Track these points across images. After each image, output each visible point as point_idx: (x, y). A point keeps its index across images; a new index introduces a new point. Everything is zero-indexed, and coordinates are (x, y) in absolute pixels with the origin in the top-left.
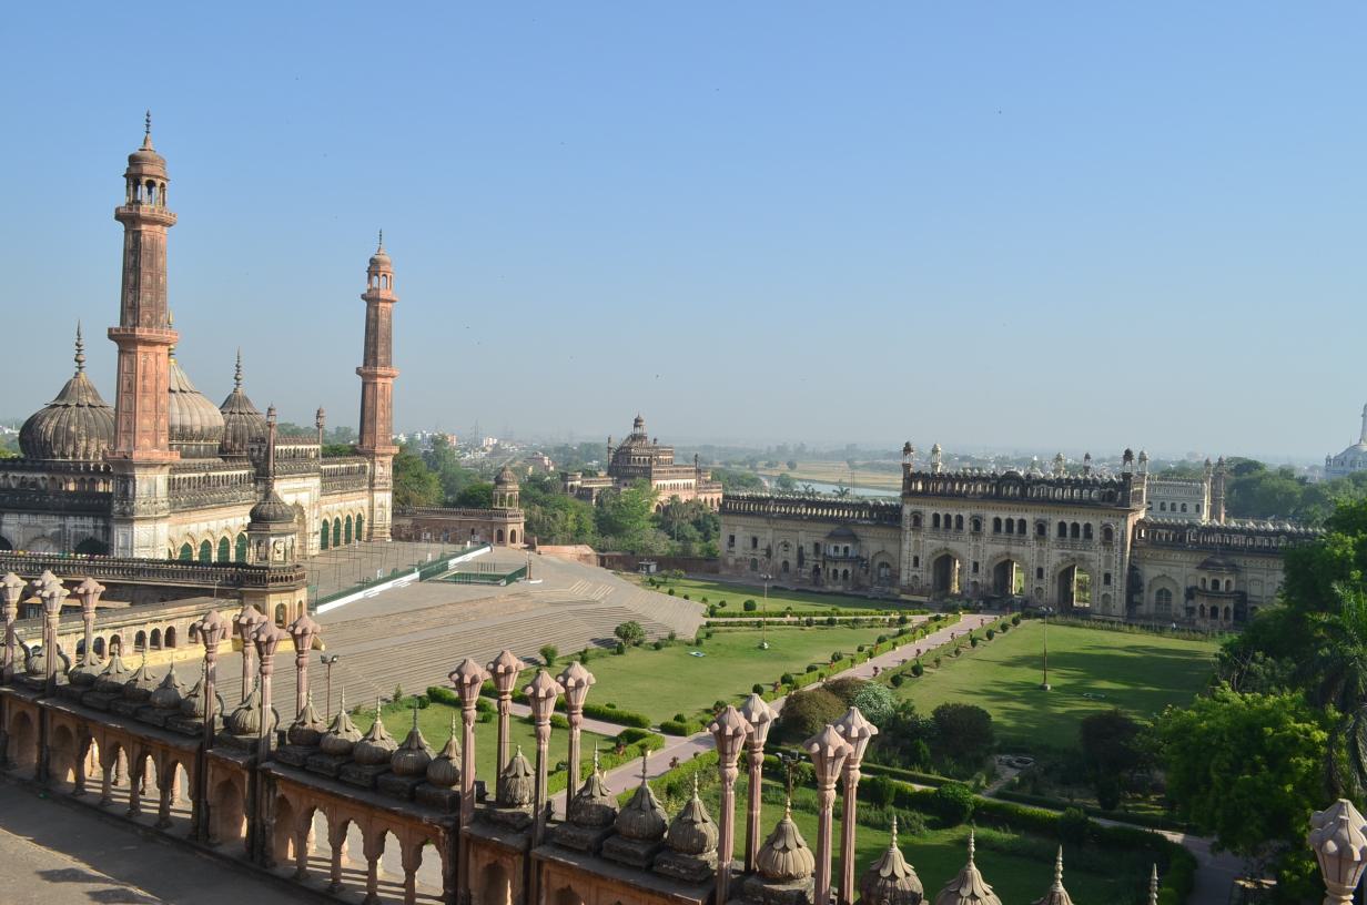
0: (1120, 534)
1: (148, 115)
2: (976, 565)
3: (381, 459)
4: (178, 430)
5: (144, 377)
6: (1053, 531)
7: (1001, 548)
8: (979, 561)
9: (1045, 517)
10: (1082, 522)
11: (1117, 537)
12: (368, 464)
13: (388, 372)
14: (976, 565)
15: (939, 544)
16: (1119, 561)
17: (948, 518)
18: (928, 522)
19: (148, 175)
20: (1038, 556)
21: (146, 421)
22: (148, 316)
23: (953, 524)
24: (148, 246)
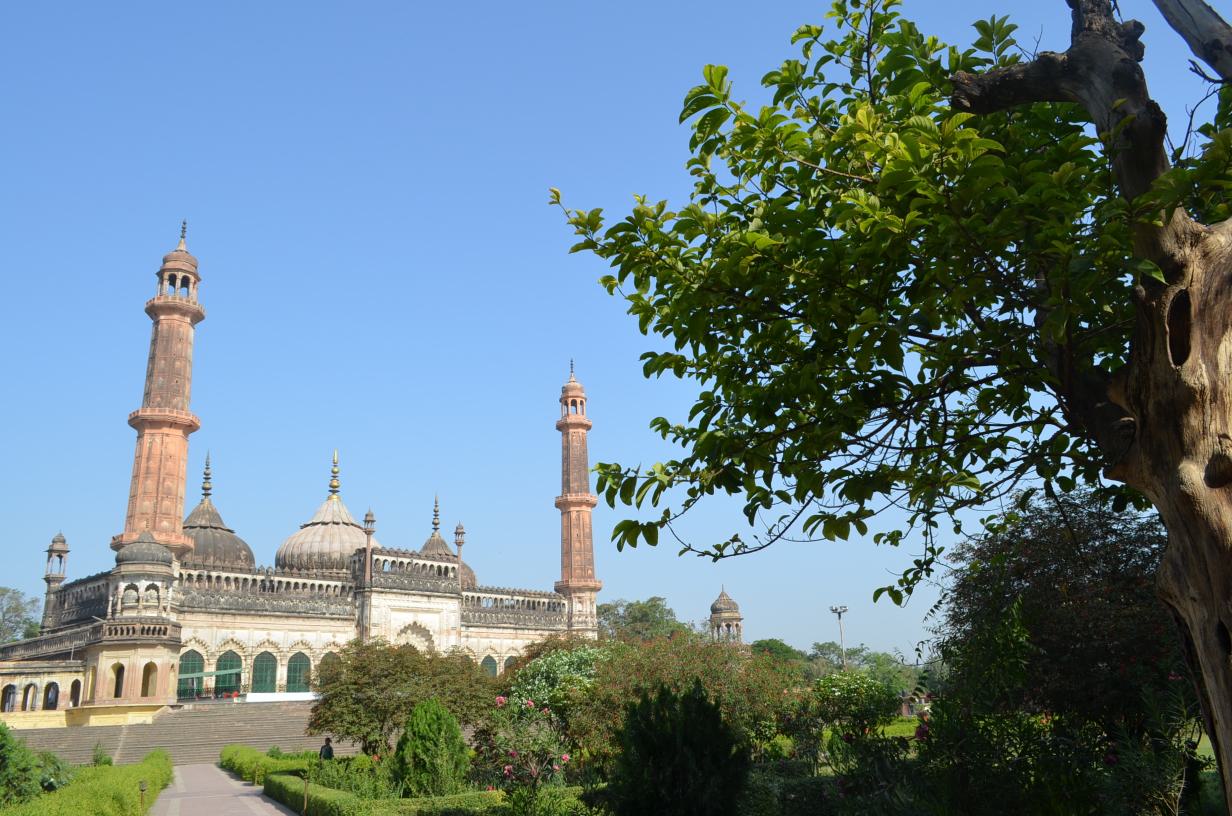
1: (185, 223)
3: (578, 595)
4: (316, 557)
5: (148, 459)
12: (566, 602)
13: (580, 497)
19: (170, 270)
21: (146, 503)
22: (159, 399)
24: (165, 334)
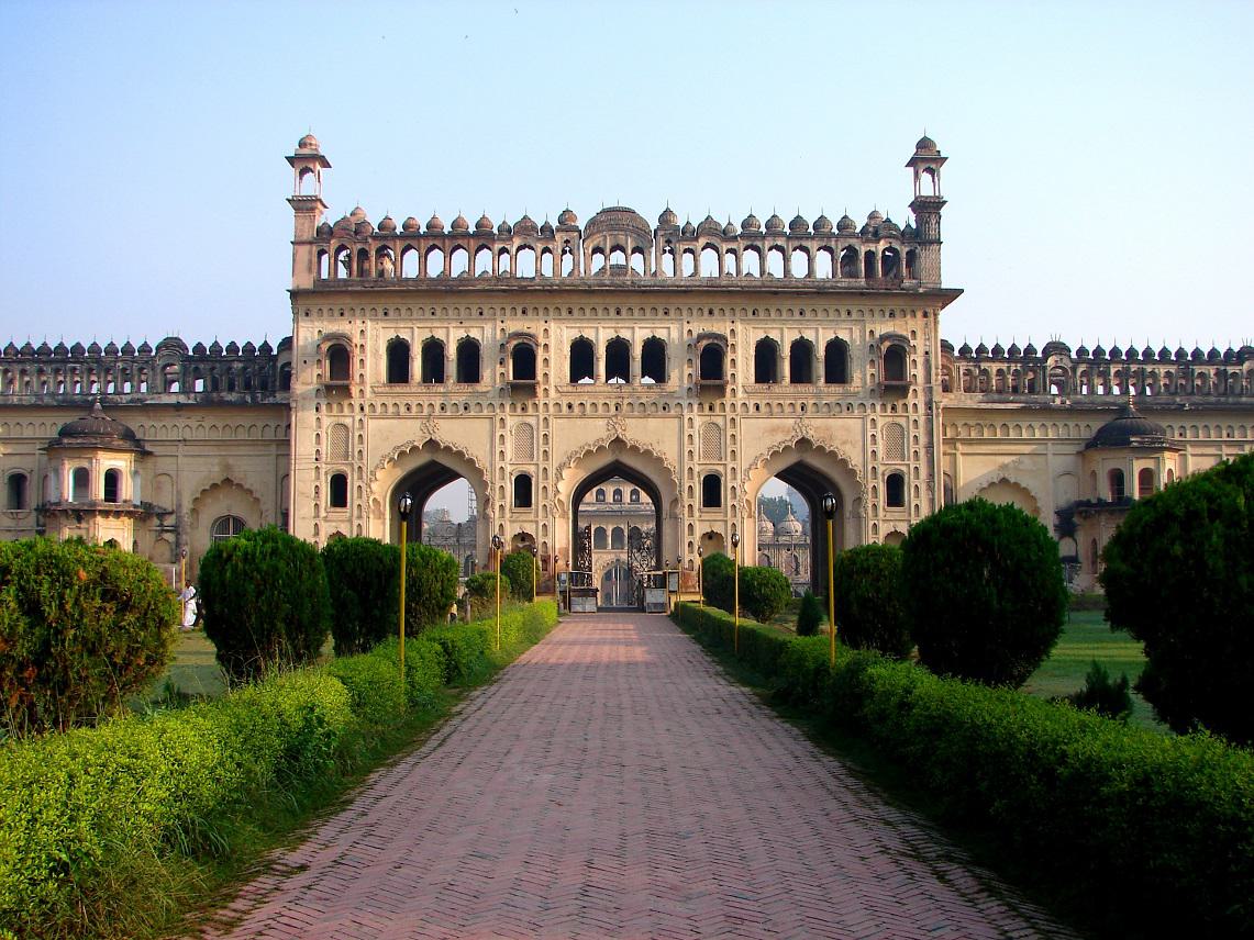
0: (920, 360)
2: (523, 487)
6: (741, 365)
7: (595, 431)
8: (531, 470)
9: (720, 327)
10: (820, 337)
11: (915, 370)
14: (523, 487)
15: (410, 432)
16: (923, 440)
17: (434, 350)
18: (371, 365)
20: (707, 440)
23: (451, 367)
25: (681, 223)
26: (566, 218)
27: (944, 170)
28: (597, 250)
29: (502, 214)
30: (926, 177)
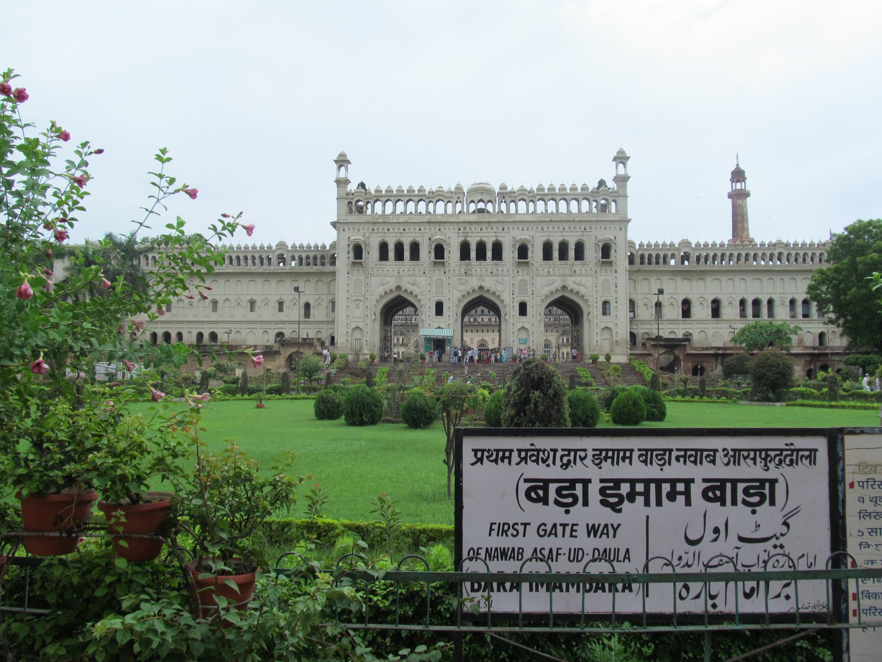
6: (536, 253)
25: (509, 189)
26: (459, 189)
27: (628, 163)
28: (472, 201)
29: (430, 186)
30: (621, 166)
